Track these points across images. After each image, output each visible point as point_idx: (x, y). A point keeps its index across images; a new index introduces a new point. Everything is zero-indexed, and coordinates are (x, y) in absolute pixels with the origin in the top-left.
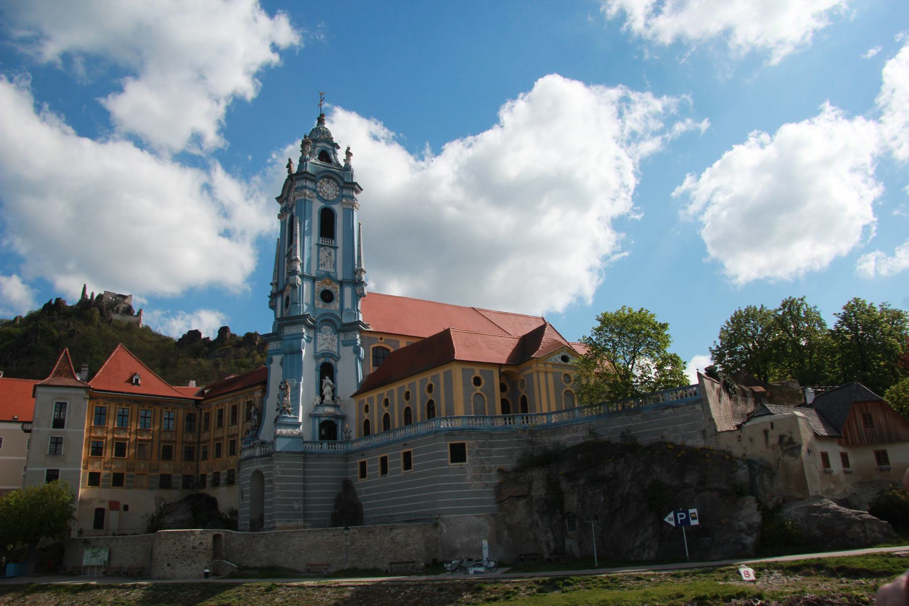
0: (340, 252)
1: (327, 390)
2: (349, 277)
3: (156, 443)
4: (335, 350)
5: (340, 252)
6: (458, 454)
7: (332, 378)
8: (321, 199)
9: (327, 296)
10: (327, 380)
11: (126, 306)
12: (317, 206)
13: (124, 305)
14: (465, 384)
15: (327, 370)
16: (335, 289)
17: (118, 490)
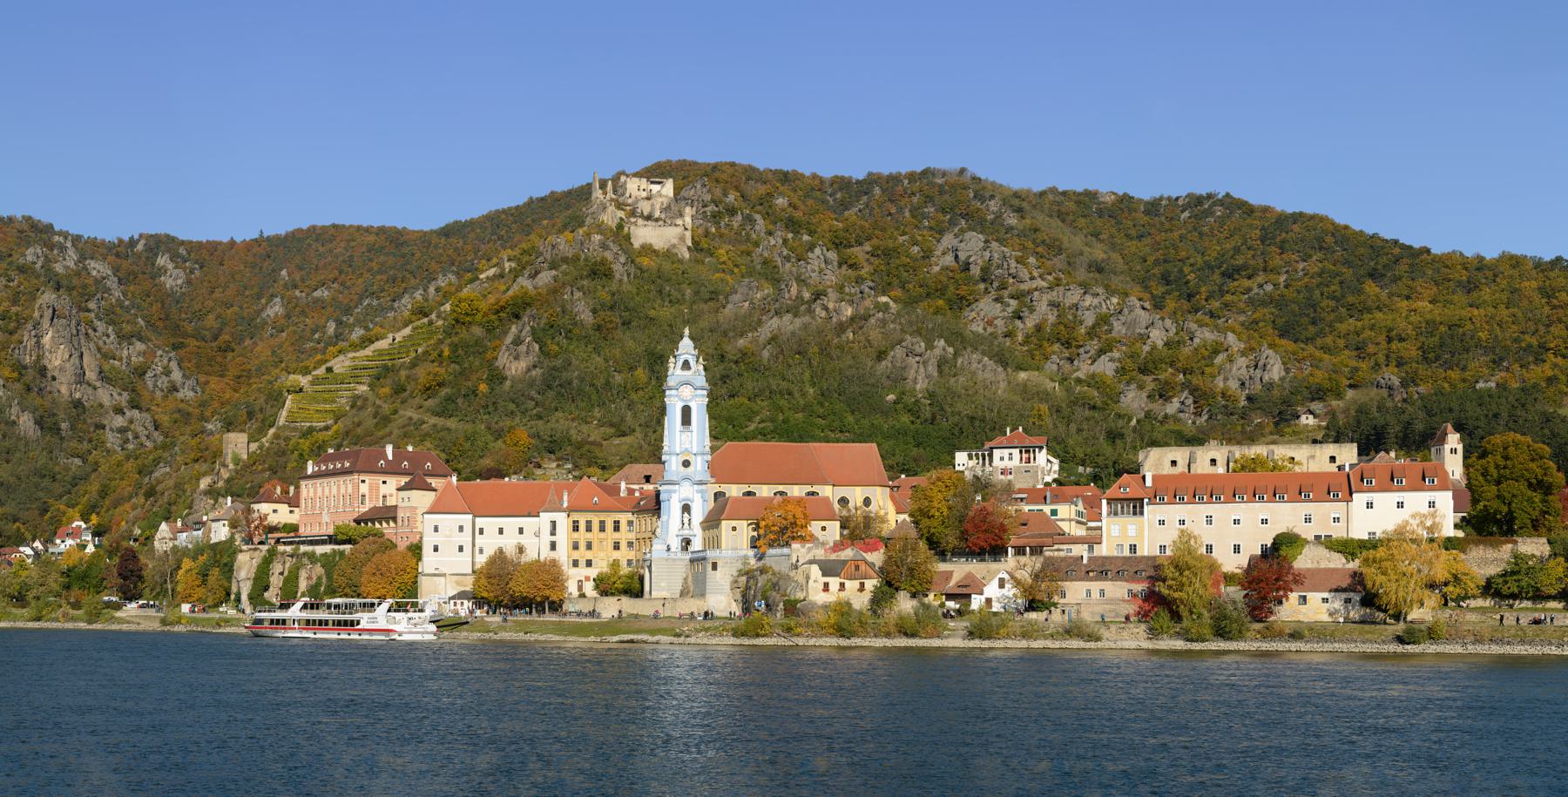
0: (695, 434)
1: (686, 521)
2: (701, 450)
3: (609, 540)
4: (691, 496)
5: (695, 434)
6: (715, 566)
7: (689, 514)
8: (684, 401)
9: (686, 464)
10: (686, 515)
11: (665, 201)
12: (679, 406)
13: (661, 200)
14: (726, 531)
15: (686, 509)
16: (692, 459)
17: (589, 569)
